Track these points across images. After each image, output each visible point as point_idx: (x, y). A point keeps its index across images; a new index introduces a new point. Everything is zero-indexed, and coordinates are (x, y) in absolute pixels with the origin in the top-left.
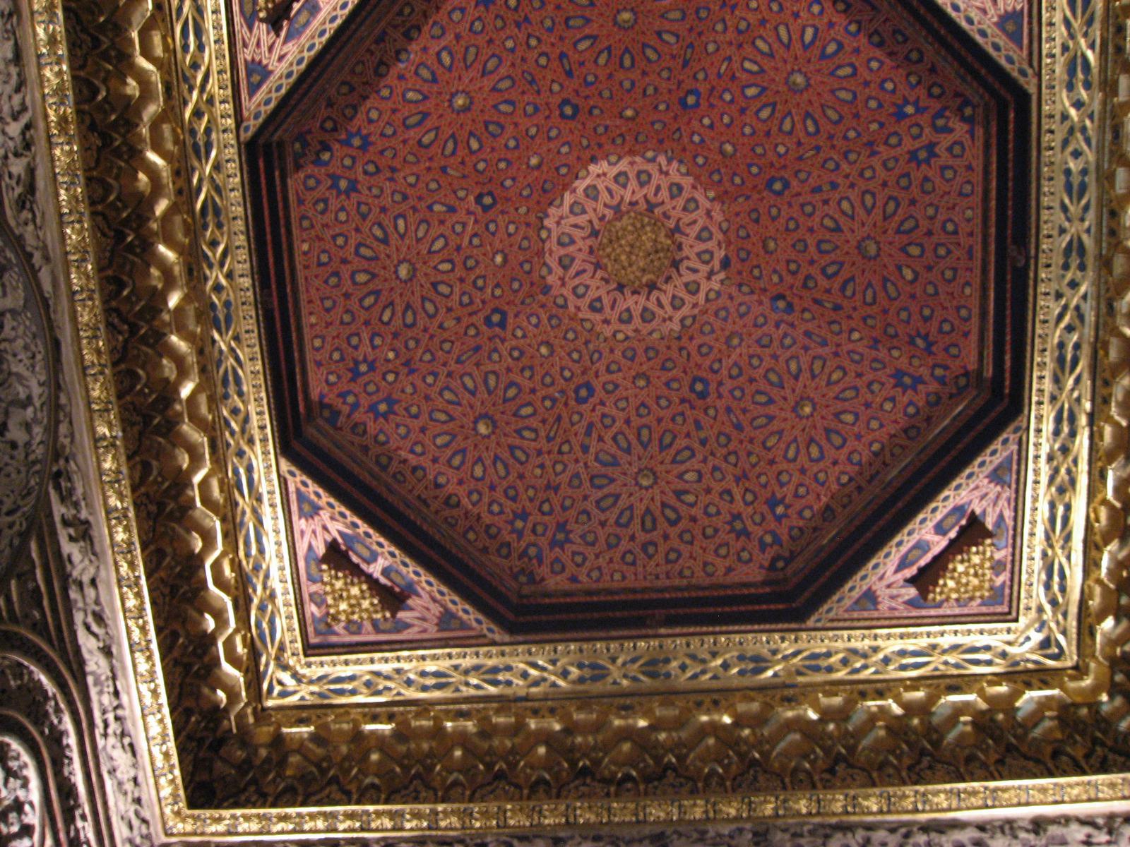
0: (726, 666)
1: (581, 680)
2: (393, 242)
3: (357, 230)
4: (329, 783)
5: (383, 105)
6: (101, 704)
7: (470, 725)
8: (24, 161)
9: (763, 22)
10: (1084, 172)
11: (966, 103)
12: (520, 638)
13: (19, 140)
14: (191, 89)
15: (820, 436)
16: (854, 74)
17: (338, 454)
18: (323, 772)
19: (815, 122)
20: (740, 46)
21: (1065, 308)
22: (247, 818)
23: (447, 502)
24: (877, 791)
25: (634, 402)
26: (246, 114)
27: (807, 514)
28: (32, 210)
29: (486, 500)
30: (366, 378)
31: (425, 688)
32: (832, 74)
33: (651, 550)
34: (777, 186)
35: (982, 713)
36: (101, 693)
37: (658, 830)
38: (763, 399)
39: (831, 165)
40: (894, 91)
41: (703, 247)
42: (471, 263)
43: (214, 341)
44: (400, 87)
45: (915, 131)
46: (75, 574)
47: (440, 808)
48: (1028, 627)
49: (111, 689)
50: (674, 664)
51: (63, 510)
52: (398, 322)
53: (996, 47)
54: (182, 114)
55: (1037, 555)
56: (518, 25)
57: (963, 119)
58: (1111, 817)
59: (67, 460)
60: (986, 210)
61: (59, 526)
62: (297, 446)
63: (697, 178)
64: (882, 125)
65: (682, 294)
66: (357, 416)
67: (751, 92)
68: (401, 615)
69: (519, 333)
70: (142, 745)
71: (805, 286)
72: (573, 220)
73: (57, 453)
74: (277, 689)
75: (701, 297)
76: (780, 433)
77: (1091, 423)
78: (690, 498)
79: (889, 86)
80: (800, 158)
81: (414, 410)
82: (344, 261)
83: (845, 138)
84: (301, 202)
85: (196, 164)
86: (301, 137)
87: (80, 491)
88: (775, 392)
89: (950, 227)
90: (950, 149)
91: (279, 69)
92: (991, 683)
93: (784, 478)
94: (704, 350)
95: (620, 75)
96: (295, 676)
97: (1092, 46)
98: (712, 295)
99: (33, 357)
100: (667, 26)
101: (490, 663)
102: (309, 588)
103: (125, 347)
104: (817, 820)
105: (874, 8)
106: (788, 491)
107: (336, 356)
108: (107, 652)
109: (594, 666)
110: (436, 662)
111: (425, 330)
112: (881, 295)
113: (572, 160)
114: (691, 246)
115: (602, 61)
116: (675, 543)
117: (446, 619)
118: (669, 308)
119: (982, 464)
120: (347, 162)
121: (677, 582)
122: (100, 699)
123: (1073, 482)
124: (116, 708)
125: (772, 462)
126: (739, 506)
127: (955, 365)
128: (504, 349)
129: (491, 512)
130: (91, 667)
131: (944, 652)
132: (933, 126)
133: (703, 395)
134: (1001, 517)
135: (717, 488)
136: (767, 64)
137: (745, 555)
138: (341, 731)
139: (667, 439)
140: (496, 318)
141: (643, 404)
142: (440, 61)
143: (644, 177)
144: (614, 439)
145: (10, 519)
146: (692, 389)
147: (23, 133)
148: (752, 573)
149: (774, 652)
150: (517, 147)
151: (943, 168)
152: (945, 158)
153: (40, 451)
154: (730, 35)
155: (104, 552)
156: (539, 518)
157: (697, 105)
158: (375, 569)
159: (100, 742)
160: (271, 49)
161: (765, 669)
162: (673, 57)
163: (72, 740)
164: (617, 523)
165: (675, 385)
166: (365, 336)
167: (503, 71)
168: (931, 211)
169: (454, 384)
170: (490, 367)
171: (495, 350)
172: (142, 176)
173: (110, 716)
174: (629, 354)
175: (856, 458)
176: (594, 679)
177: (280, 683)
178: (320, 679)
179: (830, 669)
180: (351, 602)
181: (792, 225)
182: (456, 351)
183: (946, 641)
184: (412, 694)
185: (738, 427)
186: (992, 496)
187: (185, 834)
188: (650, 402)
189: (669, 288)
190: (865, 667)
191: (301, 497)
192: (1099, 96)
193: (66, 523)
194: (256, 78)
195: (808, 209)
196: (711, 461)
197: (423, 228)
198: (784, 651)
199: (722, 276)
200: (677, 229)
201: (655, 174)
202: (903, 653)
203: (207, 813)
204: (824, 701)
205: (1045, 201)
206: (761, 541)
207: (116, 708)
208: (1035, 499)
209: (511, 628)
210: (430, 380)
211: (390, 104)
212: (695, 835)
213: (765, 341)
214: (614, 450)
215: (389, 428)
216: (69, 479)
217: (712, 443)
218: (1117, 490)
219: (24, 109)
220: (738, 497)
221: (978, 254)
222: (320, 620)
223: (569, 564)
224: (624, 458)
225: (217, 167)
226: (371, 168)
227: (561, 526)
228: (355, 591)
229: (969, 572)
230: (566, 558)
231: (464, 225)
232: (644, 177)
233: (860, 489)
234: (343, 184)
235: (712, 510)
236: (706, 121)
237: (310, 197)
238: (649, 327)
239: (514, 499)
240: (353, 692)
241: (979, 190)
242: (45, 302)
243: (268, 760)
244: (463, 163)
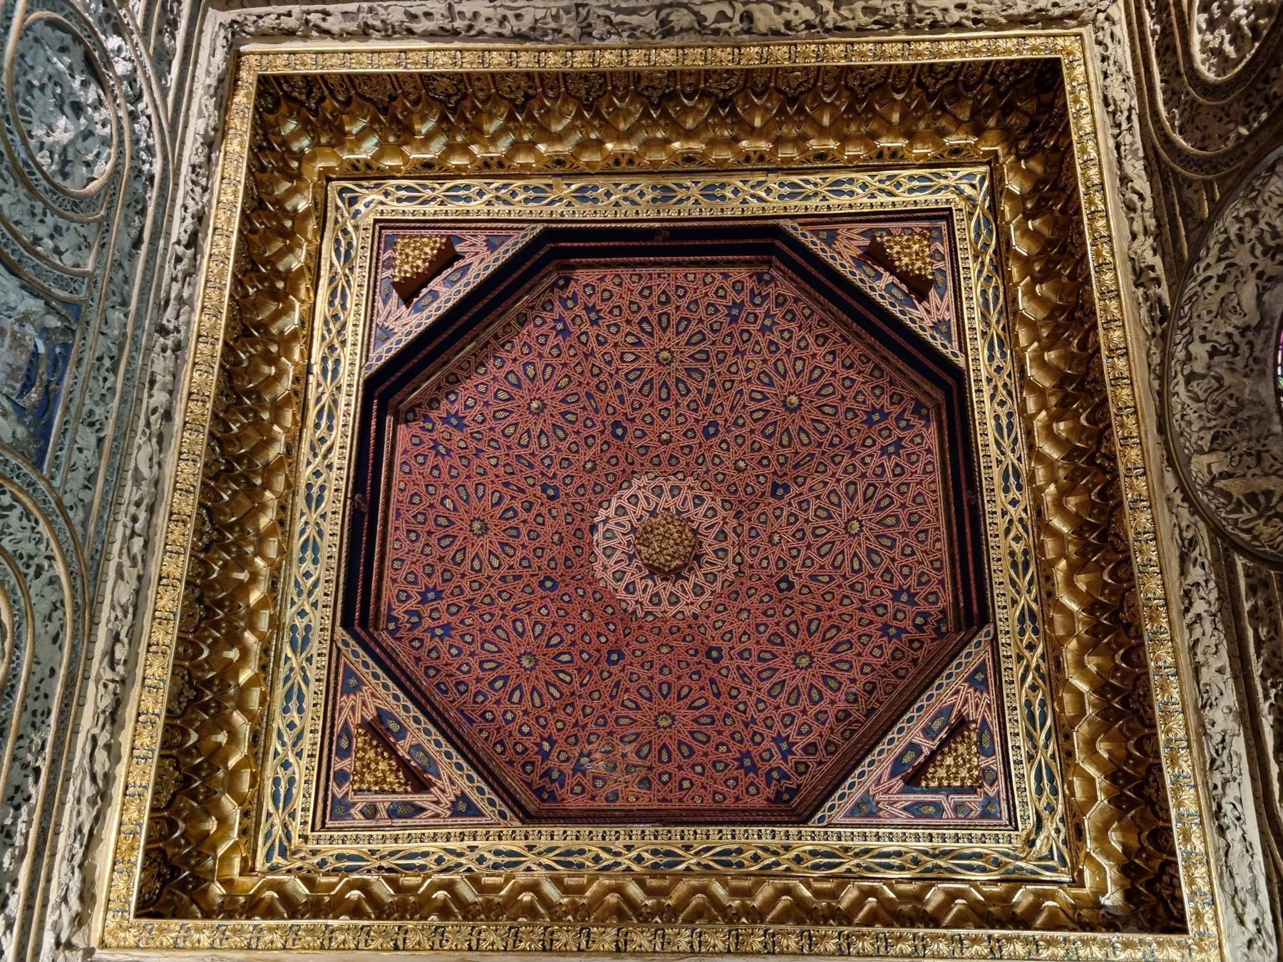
0: (608, 194)
1: (723, 186)
2: (863, 550)
3: (893, 560)
4: (935, 94)
5: (870, 659)
7: (814, 144)
8: (1190, 580)
9: (553, 710)
10: (302, 560)
11: (392, 633)
12: (770, 222)
13: (1195, 595)
14: (1038, 668)
15: (526, 383)
16: (482, 663)
17: (915, 376)
18: (940, 106)
19: (515, 629)
20: (573, 694)
21: (325, 457)
22: (1008, 51)
23: (826, 339)
24: (492, 69)
25: (671, 420)
26: (989, 648)
27: (539, 321)
28: (1183, 539)
29: (794, 342)
30: (889, 441)
31: (851, 181)
32: (499, 665)
33: (663, 298)
34: (549, 584)
35: (406, 143)
37: (667, 41)
38: (569, 417)
39: (505, 595)
40: (451, 646)
41: (611, 543)
42: (799, 535)
43: (1019, 459)
44: (855, 673)
45: (435, 615)
46: (1151, 240)
47: (843, 63)
48: (367, 215)
50: (648, 197)
51: (1159, 291)
52: (861, 486)
53: (365, 665)
54: (1045, 647)
55: (357, 270)
56: (753, 721)
57: (396, 620)
58: (306, 37)
59: (1154, 334)
60: (383, 545)
61: (1163, 277)
62: (950, 380)
63: (613, 597)
64: (462, 622)
65: (629, 507)
66: (897, 410)
67: (565, 658)
68: (867, 242)
69: (762, 479)
70: (1098, 107)
71: (531, 504)
72: (715, 569)
73: (1164, 339)
74: (976, 182)
75: (614, 503)
76: (557, 388)
77: (309, 366)
78: (630, 339)
79: (454, 651)
80: (529, 603)
81: (850, 415)
82: (905, 534)
83: (492, 615)
84: (941, 582)
85: (1034, 606)
86: (940, 635)
87: (1144, 311)
88: (560, 422)
89: (413, 536)
90: (409, 597)
91: (957, 682)
92: (397, 169)
93: (555, 352)
94: (614, 461)
95: (671, 678)
96: (960, 192)
97: (287, 659)
98: (605, 504)
99: (1183, 417)
100: (631, 714)
101: (796, 202)
102: (946, 265)
103: (1099, 444)
104: (541, 46)
105: (462, 712)
106: (552, 341)
107: (914, 458)
108: (1124, 179)
109: (713, 197)
110: (839, 203)
111: (838, 481)
112: (471, 490)
113: (714, 616)
114: (620, 541)
115: (685, 690)
116: (644, 304)
117: (831, 238)
118: (641, 496)
119: (399, 342)
120: (900, 616)
121: (644, 271)
122: (1134, 140)
123: (326, 323)
125: (564, 365)
126: (593, 331)
127: (415, 427)
128: (775, 466)
129: (790, 332)
130: (1140, 165)
131: (434, 199)
132: (420, 617)
133: (616, 424)
134: (385, 303)
135: (609, 348)
136: (551, 677)
137: (589, 291)
138: (924, 142)
139: (647, 388)
140: (780, 492)
141: (664, 418)
142: (820, 692)
143: (655, 600)
144: (689, 391)
145: (1209, 273)
146: (625, 429)
147: (1191, 604)
148: (583, 276)
149: (569, 204)
150: (758, 625)
151: (415, 583)
152: (414, 591)
153: (1178, 338)
154: (579, 703)
155: (1123, 263)
156: (751, 328)
157: (610, 653)
158: (888, 278)
159: (1135, 102)
160: (966, 701)
161: (577, 191)
162: (627, 690)
163: (1160, 97)
164: (689, 321)
165: (638, 433)
166: (889, 474)
167: (767, 685)
168: (427, 550)
169: (816, 437)
170: (787, 451)
171: (781, 465)
172: (1083, 588)
174: (674, 461)
175: (498, 363)
176: (712, 187)
177: (973, 186)
178: (939, 190)
179: (526, 188)
180: (910, 251)
181: (539, 552)
182: (814, 464)
183: (432, 208)
184: (864, 177)
185: (589, 396)
186: (391, 318)
187: (1064, 35)
188: (658, 420)
189: (639, 512)
190: (497, 189)
191: (948, 336)
192: (287, 620)
193: (1157, 281)
194: (979, 677)
195: (525, 563)
196: (612, 369)
197: (837, 563)
198: (563, 205)
199: (596, 520)
200: (631, 557)
201: (646, 602)
202: (468, 199)
203: (1043, 55)
204: (530, 160)
205: (337, 540)
206: (576, 304)
208: (357, 313)
209: (777, 232)
210: (836, 440)
211: (863, 660)
212: (638, 33)
213: (565, 464)
214: (689, 382)
215: (871, 400)
216: (1152, 318)
217: (611, 385)
218: (292, 308)
219: (1190, 627)
220: (593, 339)
221: (392, 513)
222: (935, 239)
223: (729, 289)
224: (682, 375)
225: (1014, 602)
226: (880, 611)
227: (734, 320)
228: (905, 260)
229: (412, 257)
230: (732, 295)
231: (803, 566)
232: (655, 600)
233: (496, 337)
234: (904, 597)
235: (613, 329)
236: (603, 639)
237: (935, 588)
238: (657, 482)
239: (771, 342)
240: (911, 178)
241: (387, 563)
242: (1171, 463)
243: (988, 117)
244: (803, 614)
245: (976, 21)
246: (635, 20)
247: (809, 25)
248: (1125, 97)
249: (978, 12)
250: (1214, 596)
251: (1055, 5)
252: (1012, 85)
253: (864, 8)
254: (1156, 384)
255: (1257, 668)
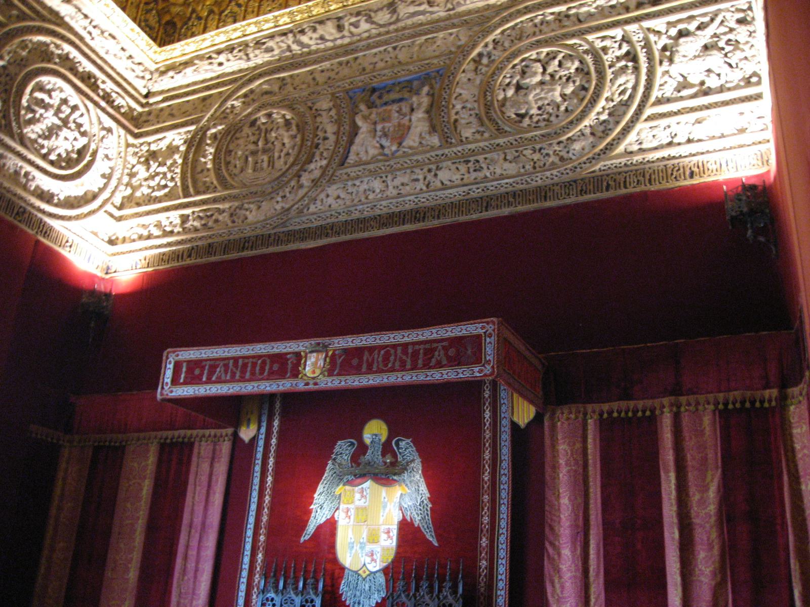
49: (82, 16)
122: (78, 24)
124: (90, 23)
159: (92, 43)
173: (90, 28)
207: (90, 23)
245: (210, 58)
246: (412, 9)
247: (302, 32)
248: (99, 44)
249: (211, 63)
251: (172, 77)
252: (189, 19)
253: (272, 50)
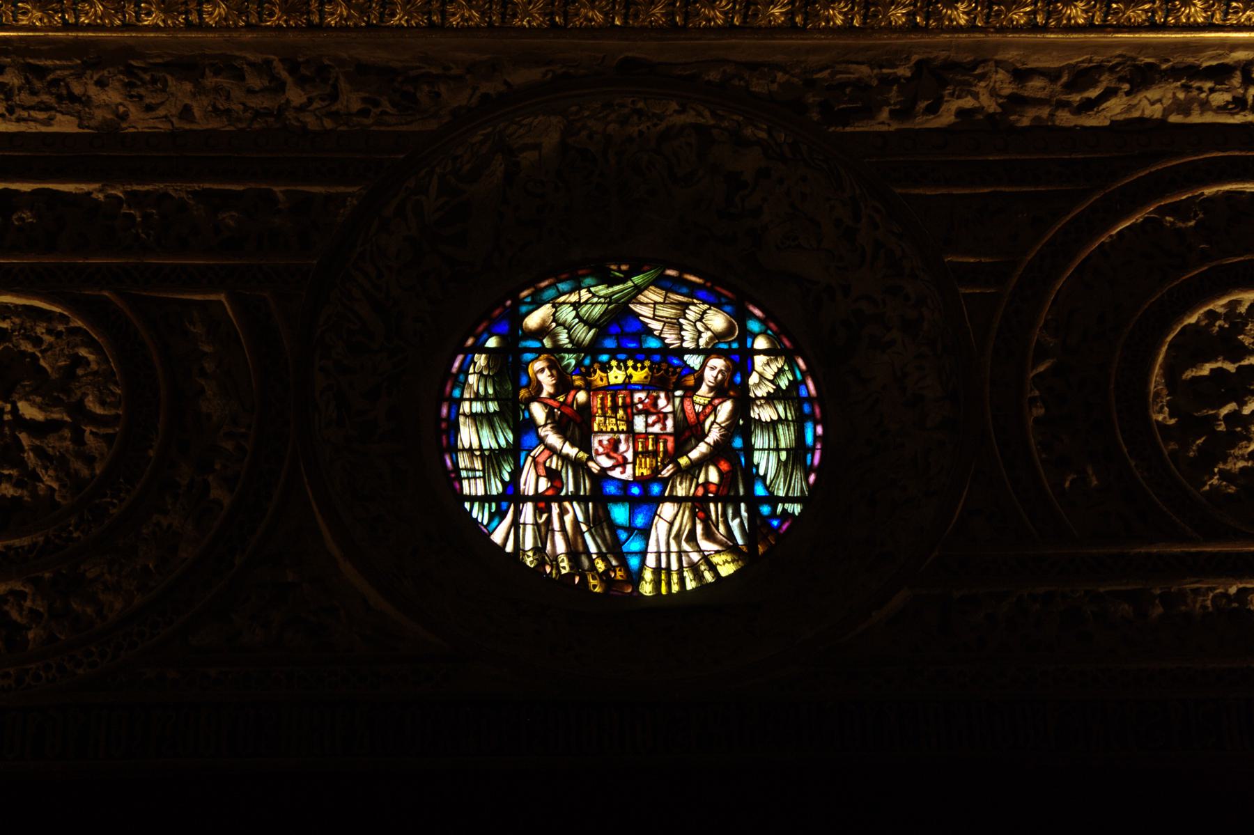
6: (1222, 109)
36: (1205, 106)
51: (885, 114)
99: (640, 112)
122: (1215, 107)
130: (1156, 111)
147: (302, 81)
155: (979, 46)
250: (310, 121)
254: (713, 76)
255: (178, 189)
